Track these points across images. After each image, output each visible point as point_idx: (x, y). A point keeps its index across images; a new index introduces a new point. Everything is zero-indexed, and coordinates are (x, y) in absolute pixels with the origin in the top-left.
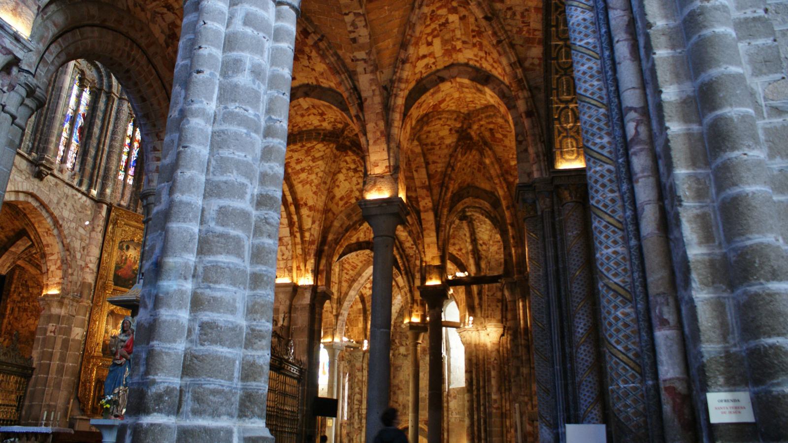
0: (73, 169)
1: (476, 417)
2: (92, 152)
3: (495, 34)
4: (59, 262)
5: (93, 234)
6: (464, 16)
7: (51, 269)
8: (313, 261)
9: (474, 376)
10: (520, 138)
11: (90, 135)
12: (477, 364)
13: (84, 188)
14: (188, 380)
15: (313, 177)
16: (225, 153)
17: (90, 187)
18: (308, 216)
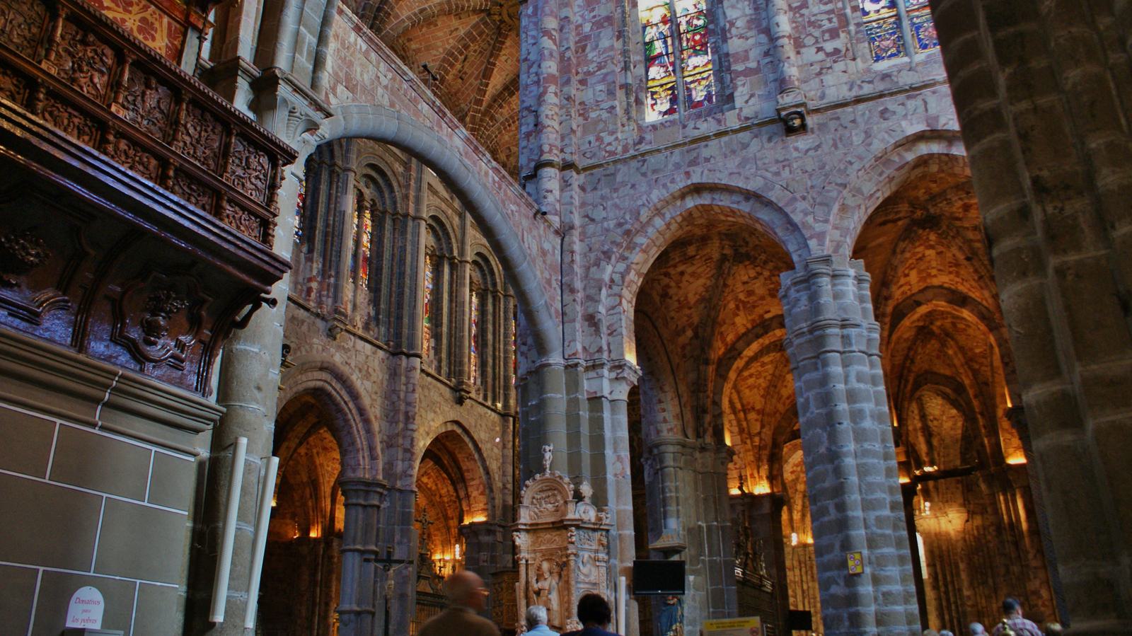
0: (475, 383)
1: (947, 617)
2: (490, 361)
3: (976, 271)
4: (481, 486)
5: (506, 451)
6: (942, 252)
7: (473, 495)
8: (766, 467)
9: (939, 570)
10: (1006, 360)
11: (485, 344)
12: (940, 557)
13: (489, 403)
14: (882, 629)
15: (761, 381)
16: (870, 479)
17: (494, 401)
18: (756, 420)
